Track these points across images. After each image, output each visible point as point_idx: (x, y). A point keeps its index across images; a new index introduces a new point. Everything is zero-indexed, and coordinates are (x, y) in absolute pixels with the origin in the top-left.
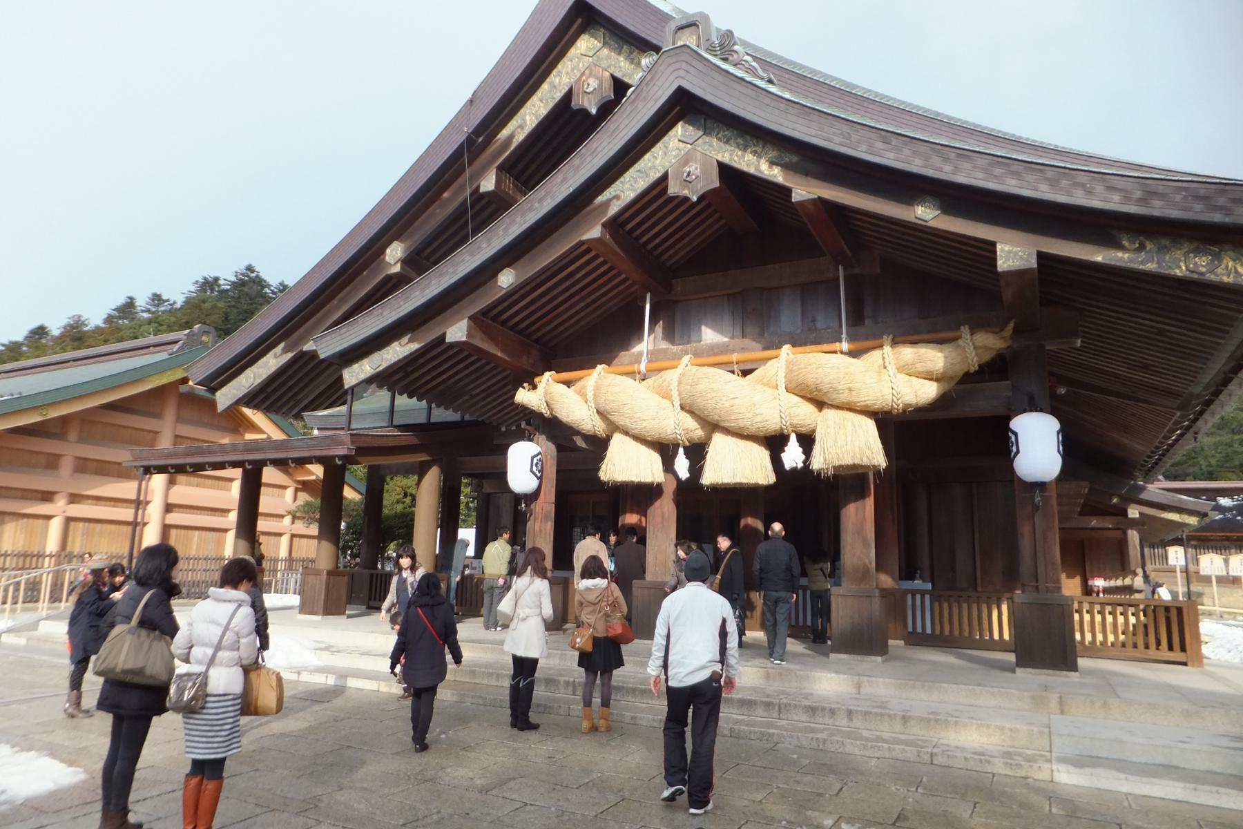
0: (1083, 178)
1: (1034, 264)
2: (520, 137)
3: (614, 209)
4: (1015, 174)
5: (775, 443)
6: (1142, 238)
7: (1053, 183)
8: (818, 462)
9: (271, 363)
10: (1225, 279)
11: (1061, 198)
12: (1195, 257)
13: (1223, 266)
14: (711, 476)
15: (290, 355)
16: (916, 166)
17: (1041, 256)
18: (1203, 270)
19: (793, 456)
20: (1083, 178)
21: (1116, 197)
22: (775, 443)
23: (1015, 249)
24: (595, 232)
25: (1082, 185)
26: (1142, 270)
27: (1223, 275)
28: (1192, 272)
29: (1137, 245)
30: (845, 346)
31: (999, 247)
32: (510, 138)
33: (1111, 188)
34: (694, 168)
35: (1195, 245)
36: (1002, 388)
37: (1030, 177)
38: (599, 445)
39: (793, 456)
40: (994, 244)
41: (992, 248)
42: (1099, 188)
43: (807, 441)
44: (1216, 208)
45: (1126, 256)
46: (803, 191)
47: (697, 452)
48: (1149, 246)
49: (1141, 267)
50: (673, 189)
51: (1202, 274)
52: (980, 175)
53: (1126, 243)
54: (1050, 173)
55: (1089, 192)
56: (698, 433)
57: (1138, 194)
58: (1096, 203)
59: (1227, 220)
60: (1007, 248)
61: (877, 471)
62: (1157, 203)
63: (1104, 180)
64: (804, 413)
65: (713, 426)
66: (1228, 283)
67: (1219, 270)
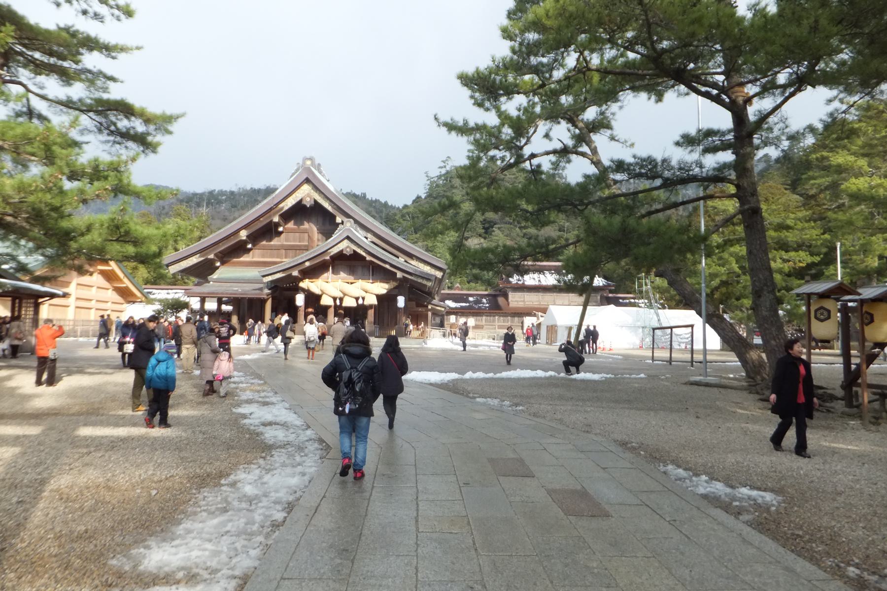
2: (286, 208)
3: (332, 254)
5: (357, 299)
8: (366, 303)
9: (194, 260)
14: (344, 304)
15: (202, 259)
16: (387, 260)
19: (360, 302)
22: (357, 299)
24: (328, 258)
30: (371, 281)
32: (282, 208)
34: (348, 249)
36: (397, 290)
38: (318, 297)
39: (360, 302)
43: (363, 299)
46: (368, 258)
47: (341, 300)
50: (344, 252)
56: (342, 295)
61: (375, 305)
64: (363, 294)
65: (345, 295)
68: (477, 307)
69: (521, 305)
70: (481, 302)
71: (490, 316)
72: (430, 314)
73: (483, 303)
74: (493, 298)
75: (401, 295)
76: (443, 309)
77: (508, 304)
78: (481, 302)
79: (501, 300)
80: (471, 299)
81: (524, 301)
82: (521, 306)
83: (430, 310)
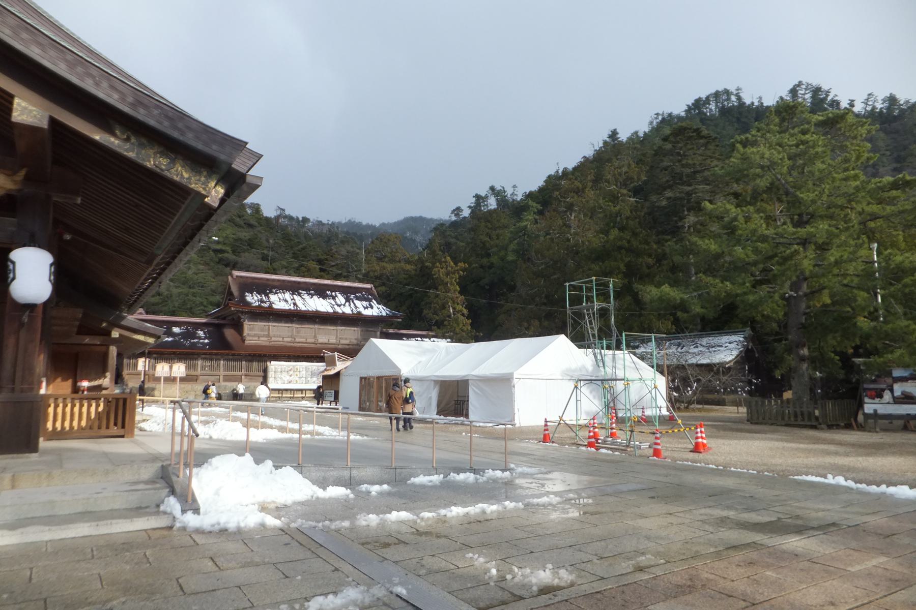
0: (95, 72)
1: (45, 124)
4: (39, 44)
6: (129, 133)
7: (71, 66)
10: (175, 178)
11: (74, 80)
12: (160, 157)
13: (175, 169)
17: (53, 121)
18: (164, 167)
20: (95, 72)
21: (116, 96)
23: (31, 108)
25: (93, 77)
26: (125, 155)
27: (175, 174)
28: (157, 167)
29: (125, 137)
31: (16, 101)
33: (112, 87)
35: (161, 149)
37: (52, 53)
40: (12, 97)
41: (10, 99)
42: (105, 84)
44: (179, 130)
45: (117, 142)
48: (133, 140)
49: (125, 153)
51: (162, 170)
52: (7, 31)
53: (118, 132)
54: (69, 57)
55: (97, 84)
57: (130, 99)
58: (101, 95)
59: (181, 138)
60: (24, 104)
62: (142, 111)
63: (108, 80)
66: (176, 181)
67: (173, 171)
68: (188, 343)
69: (263, 341)
70: (194, 336)
71: (211, 360)
72: (113, 350)
73: (200, 338)
74: (216, 329)
75: (32, 242)
76: (151, 340)
77: (243, 341)
78: (194, 336)
79: (229, 334)
80: (176, 330)
81: (268, 336)
82: (264, 343)
83: (115, 341)
